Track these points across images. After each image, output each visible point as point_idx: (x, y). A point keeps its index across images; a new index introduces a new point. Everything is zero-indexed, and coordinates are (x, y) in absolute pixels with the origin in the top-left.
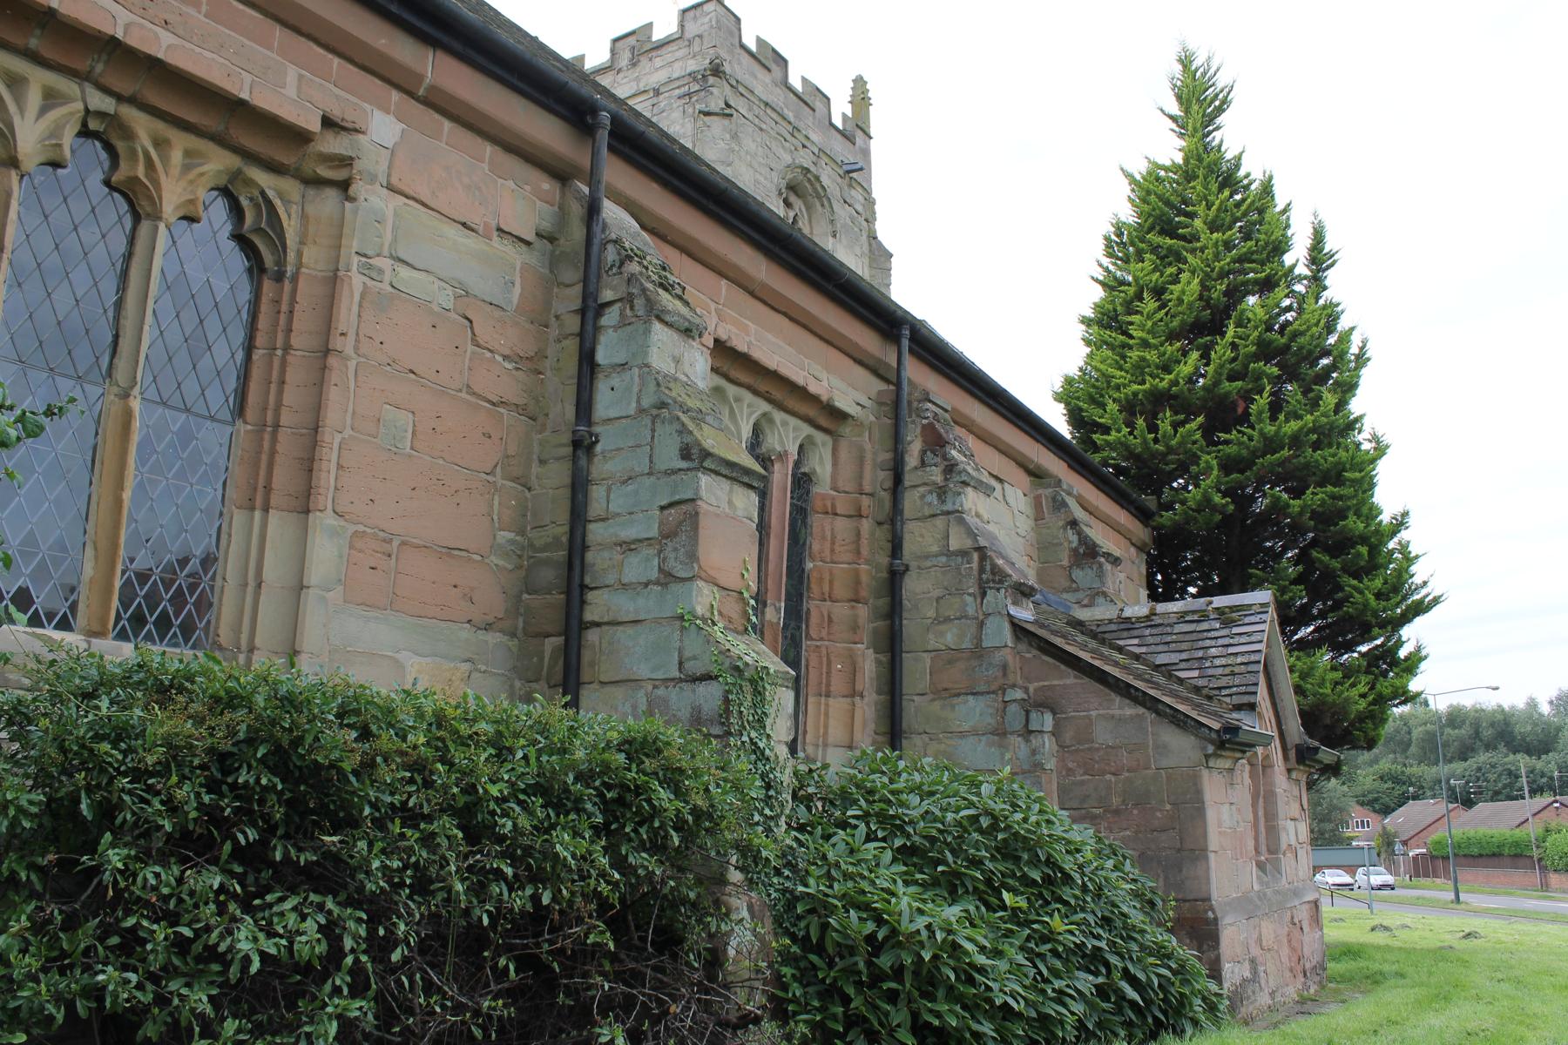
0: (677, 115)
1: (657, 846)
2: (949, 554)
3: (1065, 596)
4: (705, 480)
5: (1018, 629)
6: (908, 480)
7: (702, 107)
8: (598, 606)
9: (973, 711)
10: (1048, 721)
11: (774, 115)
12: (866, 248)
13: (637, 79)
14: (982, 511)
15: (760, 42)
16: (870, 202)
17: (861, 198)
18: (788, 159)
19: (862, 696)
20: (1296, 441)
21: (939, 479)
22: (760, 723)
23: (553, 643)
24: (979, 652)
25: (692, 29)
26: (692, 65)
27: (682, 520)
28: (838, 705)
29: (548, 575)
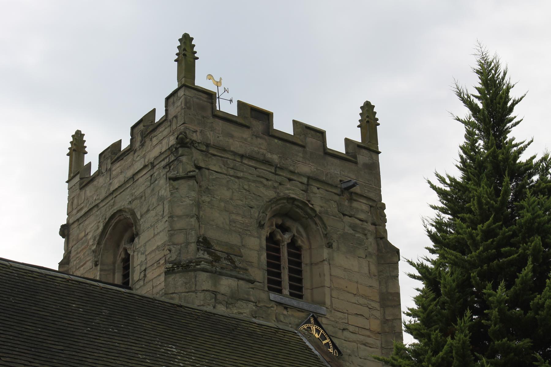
7: (172, 174)
11: (252, 163)
13: (144, 156)
15: (241, 105)
17: (365, 207)
18: (271, 194)
25: (173, 112)
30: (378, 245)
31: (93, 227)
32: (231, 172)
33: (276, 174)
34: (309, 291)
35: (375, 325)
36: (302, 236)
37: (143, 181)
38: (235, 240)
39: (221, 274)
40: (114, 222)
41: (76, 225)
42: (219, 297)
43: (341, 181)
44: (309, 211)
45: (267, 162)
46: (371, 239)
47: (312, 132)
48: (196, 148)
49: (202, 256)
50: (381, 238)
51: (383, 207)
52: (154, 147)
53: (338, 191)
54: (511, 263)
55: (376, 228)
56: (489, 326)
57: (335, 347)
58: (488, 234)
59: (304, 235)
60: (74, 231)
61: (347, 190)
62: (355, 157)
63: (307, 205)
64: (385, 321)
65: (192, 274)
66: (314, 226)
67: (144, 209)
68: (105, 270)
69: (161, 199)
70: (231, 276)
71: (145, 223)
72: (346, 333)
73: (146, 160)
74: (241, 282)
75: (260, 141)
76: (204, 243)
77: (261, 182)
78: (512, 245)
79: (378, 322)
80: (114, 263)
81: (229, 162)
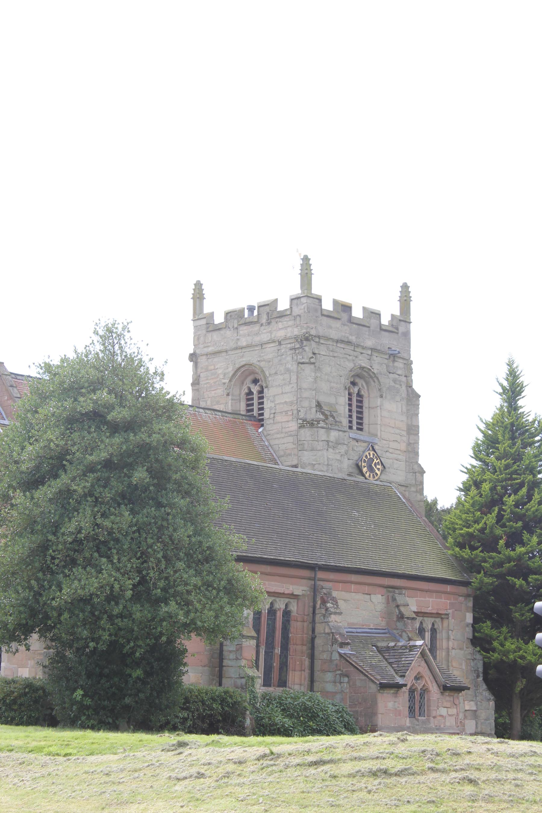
0: (289, 358)
1: (228, 706)
2: (325, 634)
3: (394, 631)
4: (244, 640)
5: (340, 655)
6: (317, 612)
8: (225, 662)
9: (329, 676)
10: (346, 679)
11: (342, 346)
12: (404, 395)
13: (271, 332)
14: (337, 620)
15: (336, 303)
16: (408, 364)
17: (401, 365)
18: (351, 365)
19: (304, 671)
20: (520, 558)
21: (324, 612)
22: (253, 686)
23: (217, 669)
24: (331, 661)
25: (296, 311)
26: (296, 332)
27: (240, 648)
28: (297, 673)
29: (216, 656)
30: (408, 391)
31: (224, 367)
32: (331, 354)
33: (354, 351)
34: (367, 426)
35: (403, 447)
36: (364, 388)
37: (271, 349)
38: (332, 400)
39: (331, 429)
40: (243, 369)
41: (204, 357)
42: (330, 444)
43: (389, 348)
44: (371, 374)
45: (349, 343)
46: (404, 388)
47: (374, 315)
48: (313, 340)
49: (319, 417)
50: (410, 387)
51: (411, 363)
52: (280, 329)
53: (387, 357)
54: (517, 484)
55: (407, 379)
56: (504, 515)
57: (382, 464)
58: (507, 467)
59: (366, 387)
60: (202, 361)
61: (393, 356)
62: (397, 329)
63: (371, 370)
64: (409, 444)
65: (316, 429)
66: (372, 383)
67: (273, 372)
68: (235, 400)
69: (288, 371)
70: (336, 430)
72: (388, 454)
73: (273, 336)
74: (341, 433)
75: (346, 327)
76: (319, 405)
77: (346, 358)
78: (518, 474)
79: (405, 444)
80: (240, 395)
81: (330, 347)
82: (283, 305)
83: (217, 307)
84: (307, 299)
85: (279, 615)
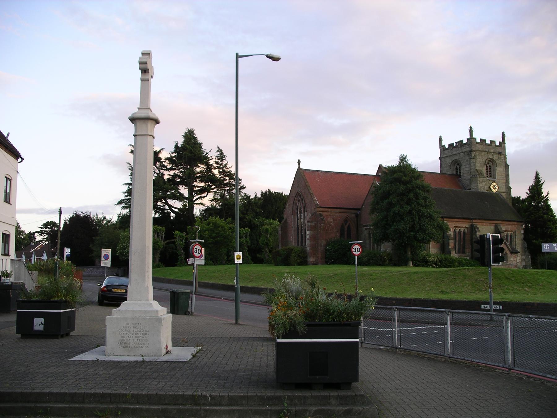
15: (481, 140)
16: (505, 156)
31: (449, 161)
35: (505, 181)
61: (500, 154)
71: (464, 164)
82: (465, 141)
83: (446, 143)
84: (471, 139)
85: (462, 233)
